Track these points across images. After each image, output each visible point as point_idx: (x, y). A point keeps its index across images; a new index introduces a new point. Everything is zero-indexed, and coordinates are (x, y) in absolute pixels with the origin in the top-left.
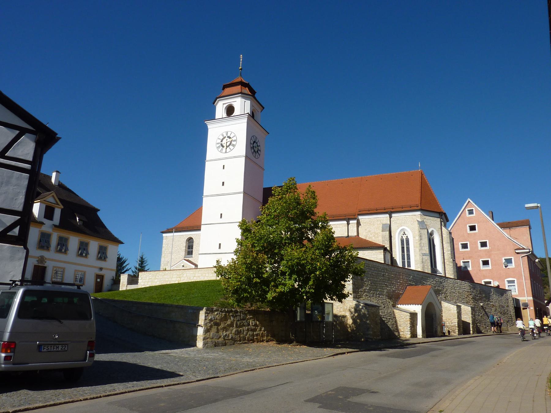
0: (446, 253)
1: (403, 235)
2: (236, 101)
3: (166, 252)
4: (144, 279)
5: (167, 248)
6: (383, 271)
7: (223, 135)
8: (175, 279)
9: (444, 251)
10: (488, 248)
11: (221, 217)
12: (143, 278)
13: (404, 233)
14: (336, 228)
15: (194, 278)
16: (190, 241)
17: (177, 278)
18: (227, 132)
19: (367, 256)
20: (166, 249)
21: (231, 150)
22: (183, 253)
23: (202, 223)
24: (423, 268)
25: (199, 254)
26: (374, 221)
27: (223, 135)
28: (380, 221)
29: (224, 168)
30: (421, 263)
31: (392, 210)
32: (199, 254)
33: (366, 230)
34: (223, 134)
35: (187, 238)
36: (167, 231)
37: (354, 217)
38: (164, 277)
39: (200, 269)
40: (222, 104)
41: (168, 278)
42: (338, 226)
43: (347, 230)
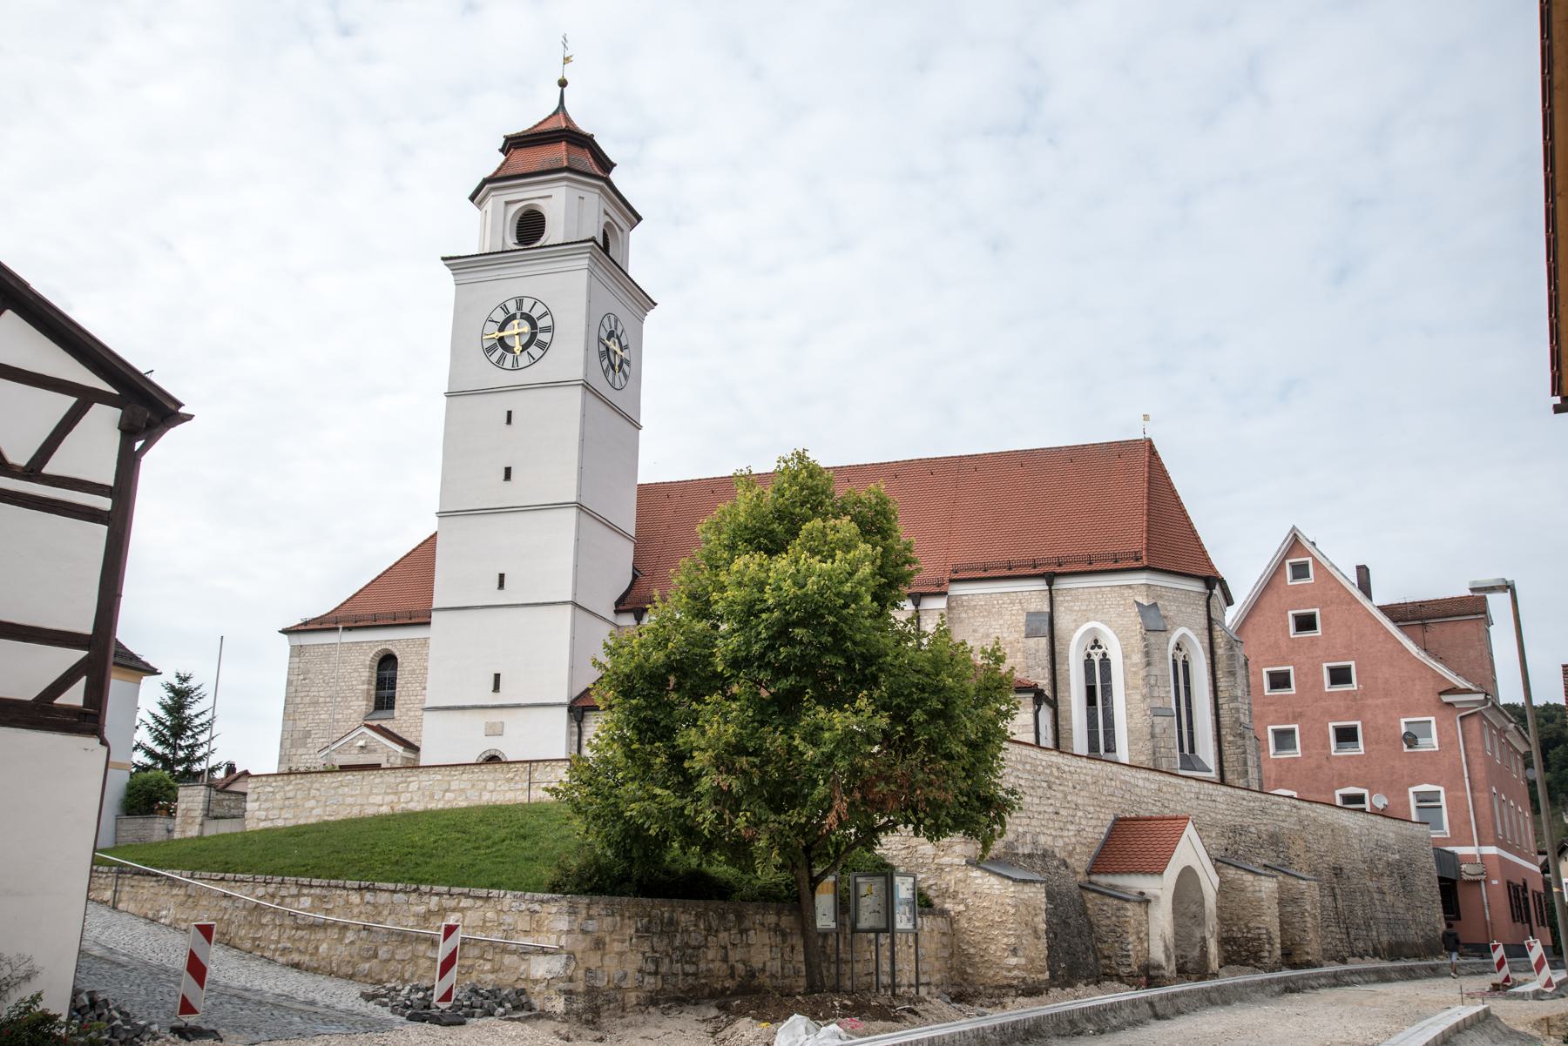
0: (1226, 706)
1: (1093, 648)
2: (550, 196)
3: (298, 700)
4: (265, 801)
5: (302, 685)
6: (1048, 771)
7: (504, 308)
8: (380, 797)
9: (1221, 701)
10: (1356, 688)
11: (501, 585)
12: (263, 797)
13: (1096, 641)
15: (447, 794)
16: (387, 662)
17: (386, 793)
18: (521, 301)
20: (299, 688)
21: (532, 361)
22: (360, 704)
23: (434, 606)
24: (1154, 753)
25: (425, 709)
27: (504, 308)
28: (1020, 603)
29: (509, 421)
30: (1149, 737)
31: (1058, 570)
32: (425, 709)
33: (975, 631)
36: (303, 628)
37: (938, 590)
38: (340, 791)
39: (468, 767)
40: (502, 205)
41: (352, 796)
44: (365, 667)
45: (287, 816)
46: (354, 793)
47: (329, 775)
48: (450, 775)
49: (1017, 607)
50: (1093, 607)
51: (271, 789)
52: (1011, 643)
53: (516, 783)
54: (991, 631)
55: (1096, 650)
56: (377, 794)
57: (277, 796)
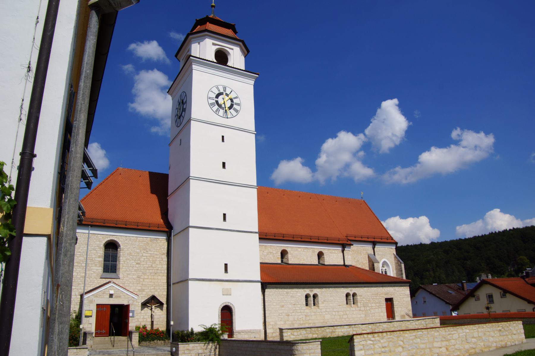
2: (232, 49)
4: (368, 350)
8: (439, 343)
11: (225, 219)
14: (332, 254)
17: (442, 341)
18: (225, 88)
21: (232, 116)
26: (361, 249)
28: (366, 250)
33: (354, 259)
34: (219, 86)
42: (334, 251)
43: (342, 258)
44: (100, 248)
46: (423, 342)
47: (408, 332)
48: (472, 329)
52: (364, 264)
53: (503, 332)
54: (359, 259)
55: (383, 268)
56: (437, 342)
57: (376, 346)
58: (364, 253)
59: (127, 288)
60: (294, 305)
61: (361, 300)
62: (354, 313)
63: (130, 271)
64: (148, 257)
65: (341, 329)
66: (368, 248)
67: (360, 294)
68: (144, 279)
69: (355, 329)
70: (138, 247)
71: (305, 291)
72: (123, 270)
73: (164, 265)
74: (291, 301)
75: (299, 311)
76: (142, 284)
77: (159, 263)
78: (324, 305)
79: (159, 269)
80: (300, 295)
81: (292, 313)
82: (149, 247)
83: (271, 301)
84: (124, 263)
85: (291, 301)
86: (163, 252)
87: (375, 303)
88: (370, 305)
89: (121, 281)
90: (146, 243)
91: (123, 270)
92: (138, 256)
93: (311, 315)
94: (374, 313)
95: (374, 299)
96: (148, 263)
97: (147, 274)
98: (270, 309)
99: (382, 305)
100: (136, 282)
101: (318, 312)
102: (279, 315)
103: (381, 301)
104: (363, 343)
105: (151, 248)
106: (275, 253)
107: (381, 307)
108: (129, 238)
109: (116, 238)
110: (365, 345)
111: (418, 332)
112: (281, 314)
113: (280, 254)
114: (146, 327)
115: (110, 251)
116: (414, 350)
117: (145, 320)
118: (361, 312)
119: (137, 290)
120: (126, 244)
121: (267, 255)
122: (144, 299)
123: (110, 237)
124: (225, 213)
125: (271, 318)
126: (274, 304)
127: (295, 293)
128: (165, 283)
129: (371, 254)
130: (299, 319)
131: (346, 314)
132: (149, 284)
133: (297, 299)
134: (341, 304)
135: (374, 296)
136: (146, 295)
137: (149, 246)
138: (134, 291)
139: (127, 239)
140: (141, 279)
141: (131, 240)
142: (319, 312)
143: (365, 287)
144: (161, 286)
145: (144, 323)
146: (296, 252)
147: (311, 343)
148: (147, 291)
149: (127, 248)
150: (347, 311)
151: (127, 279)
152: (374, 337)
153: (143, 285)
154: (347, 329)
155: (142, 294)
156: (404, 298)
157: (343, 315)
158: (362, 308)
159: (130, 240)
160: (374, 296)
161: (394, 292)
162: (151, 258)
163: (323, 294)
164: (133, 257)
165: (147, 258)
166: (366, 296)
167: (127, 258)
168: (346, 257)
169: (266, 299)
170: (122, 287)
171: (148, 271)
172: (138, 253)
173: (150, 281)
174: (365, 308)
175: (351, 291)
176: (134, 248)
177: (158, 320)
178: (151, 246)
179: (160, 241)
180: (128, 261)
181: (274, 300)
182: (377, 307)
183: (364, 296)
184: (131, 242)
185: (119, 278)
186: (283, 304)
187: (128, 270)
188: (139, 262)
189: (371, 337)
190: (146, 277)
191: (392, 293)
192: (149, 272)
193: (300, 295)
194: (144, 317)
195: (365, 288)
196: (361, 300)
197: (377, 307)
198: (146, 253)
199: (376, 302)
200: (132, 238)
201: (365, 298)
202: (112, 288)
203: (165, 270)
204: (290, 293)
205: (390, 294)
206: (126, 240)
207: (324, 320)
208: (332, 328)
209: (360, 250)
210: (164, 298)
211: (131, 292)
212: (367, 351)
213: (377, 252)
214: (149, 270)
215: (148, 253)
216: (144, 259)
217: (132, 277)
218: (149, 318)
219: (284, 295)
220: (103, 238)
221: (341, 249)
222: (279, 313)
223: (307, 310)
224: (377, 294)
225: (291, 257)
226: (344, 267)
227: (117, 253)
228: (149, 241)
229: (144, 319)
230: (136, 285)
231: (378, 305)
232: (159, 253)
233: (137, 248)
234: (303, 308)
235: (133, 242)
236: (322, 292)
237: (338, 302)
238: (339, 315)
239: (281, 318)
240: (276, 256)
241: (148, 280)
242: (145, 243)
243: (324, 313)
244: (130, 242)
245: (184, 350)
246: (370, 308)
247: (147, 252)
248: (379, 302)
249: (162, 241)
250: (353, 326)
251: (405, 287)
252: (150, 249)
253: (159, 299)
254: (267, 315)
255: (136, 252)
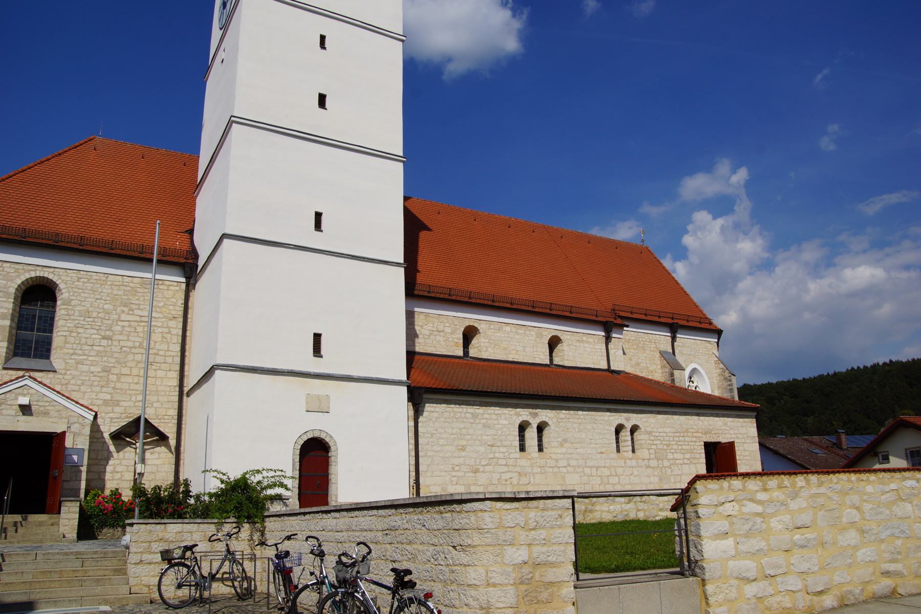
4: (748, 535)
11: (318, 226)
19: (731, 429)
28: (655, 343)
35: (23, 278)
42: (585, 338)
43: (605, 354)
45: (804, 567)
49: (653, 346)
50: (694, 353)
51: (759, 509)
54: (640, 361)
57: (774, 523)
58: (652, 349)
59: (74, 396)
60: (492, 446)
61: (651, 442)
62: (635, 473)
63: (85, 355)
64: (133, 323)
65: (606, 505)
66: (661, 338)
67: (649, 429)
68: (120, 375)
69: (641, 506)
70: (109, 299)
71: (518, 415)
72: (66, 351)
73: (174, 343)
74: (484, 437)
75: (503, 462)
76: (113, 388)
77: (160, 339)
78: (564, 450)
79: (161, 353)
80: (506, 422)
81: (486, 465)
82: (138, 299)
83: (432, 434)
84: (70, 336)
85: (484, 437)
86: (173, 312)
87: (682, 451)
88: (670, 456)
89: (58, 378)
90: (129, 288)
91: (66, 351)
92: (108, 320)
93: (534, 474)
94: (680, 475)
95: (678, 443)
96: (132, 338)
97: (129, 364)
98: (430, 454)
99: (697, 456)
100: (99, 381)
101: (548, 466)
102: (453, 468)
103: (695, 447)
104: (728, 508)
105: (142, 303)
106: (450, 331)
107: (695, 461)
108: (86, 275)
109: (52, 272)
110: (735, 517)
111: (905, 479)
112: (457, 468)
113: (461, 336)
114: (120, 495)
115: (36, 305)
116: (899, 542)
117: (119, 475)
118: (649, 471)
119: (101, 402)
120: (76, 290)
121: (429, 336)
122: (117, 424)
123: (35, 271)
124: (319, 210)
125: (431, 476)
126: (442, 442)
127: (494, 417)
128: (175, 386)
129: (666, 352)
130: (504, 482)
131: (616, 475)
132: (131, 388)
133: (500, 432)
134: (603, 450)
135: (678, 434)
136: (123, 416)
137: (137, 298)
138: (91, 404)
139: (81, 278)
140: (113, 374)
141: (92, 281)
142: (550, 467)
143: (659, 413)
144: (163, 393)
145: (115, 482)
146: (498, 334)
147: (535, 503)
148: (125, 404)
149: (78, 298)
150: (619, 467)
151: (77, 373)
152: (765, 490)
153: (117, 389)
154: (623, 506)
155: (113, 412)
156: (745, 445)
157: (609, 476)
158: (654, 463)
159: (89, 280)
160: (679, 437)
161: (725, 430)
162: (138, 325)
163: (562, 424)
164: (94, 321)
165: (130, 326)
166: (661, 434)
167: (79, 323)
168: (611, 352)
169: (420, 429)
170: (58, 392)
171: (130, 357)
172: (109, 314)
173: (136, 381)
174: (660, 462)
175: (628, 419)
176: (98, 301)
177: (153, 477)
178: (142, 299)
179: (165, 287)
180: (80, 330)
181: (440, 430)
182: (686, 461)
183: (657, 434)
184: (92, 285)
185: (55, 371)
186: (464, 442)
187: (81, 352)
188: (108, 333)
189: (756, 488)
190: (125, 371)
191: (720, 432)
192: (133, 360)
193: (506, 422)
194: (115, 468)
195: (660, 417)
196: (651, 442)
197: (686, 461)
198: (128, 314)
199: (682, 449)
200: (95, 276)
201: (658, 438)
202: (25, 392)
203: (177, 356)
204: (480, 417)
205: (715, 434)
206: (78, 281)
207: (563, 485)
208: (586, 500)
209: (642, 341)
210: (170, 425)
211: (82, 405)
212: (743, 539)
213: (679, 348)
214: (134, 354)
215: (133, 315)
216: (123, 326)
217: (89, 369)
218: (128, 471)
219: (464, 420)
220: (16, 270)
221: (603, 334)
222: (454, 464)
223: (523, 461)
224: (687, 431)
225: (487, 344)
226: (608, 373)
227: (55, 311)
228: (138, 286)
229: (115, 474)
230: (98, 389)
231: (688, 456)
232: (161, 316)
233: (105, 301)
234: (512, 456)
235: (97, 286)
236: (560, 420)
237: (597, 444)
238: (600, 476)
239: (458, 477)
240: (451, 339)
241: (129, 379)
242: (129, 291)
243: (564, 470)
244: (89, 286)
245: (150, 542)
246: (671, 461)
247: (131, 312)
248: (691, 452)
249: (171, 288)
250: (638, 498)
251: (746, 420)
252: (139, 305)
253: (156, 425)
254: (422, 468)
255: (103, 309)
